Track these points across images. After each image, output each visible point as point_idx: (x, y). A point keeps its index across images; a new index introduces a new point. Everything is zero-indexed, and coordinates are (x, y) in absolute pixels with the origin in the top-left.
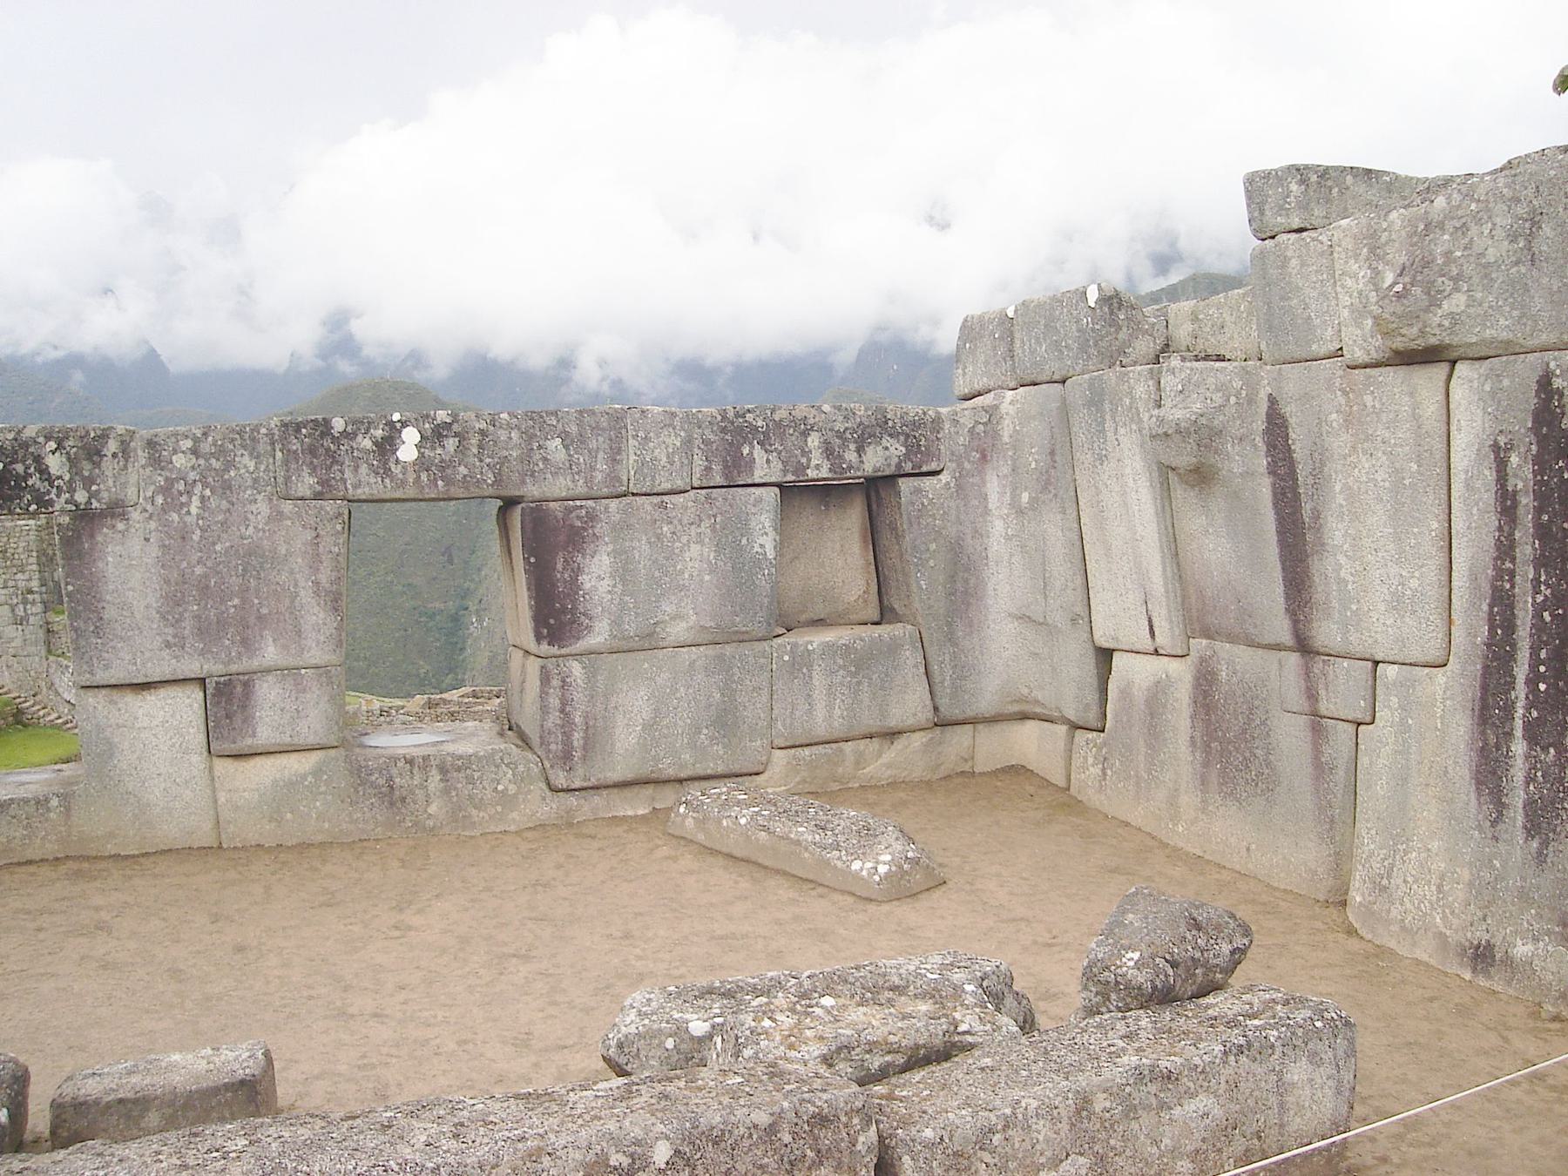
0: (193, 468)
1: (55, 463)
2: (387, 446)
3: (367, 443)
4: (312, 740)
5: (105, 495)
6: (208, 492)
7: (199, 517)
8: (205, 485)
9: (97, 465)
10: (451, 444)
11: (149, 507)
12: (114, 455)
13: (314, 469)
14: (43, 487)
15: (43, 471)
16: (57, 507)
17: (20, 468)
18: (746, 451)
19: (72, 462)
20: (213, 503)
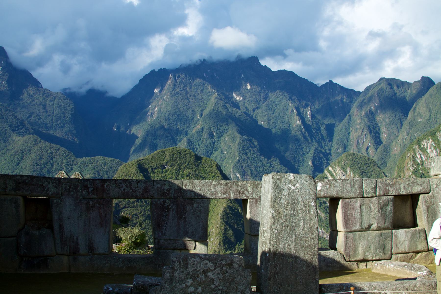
9: (257, 189)
15: (247, 190)
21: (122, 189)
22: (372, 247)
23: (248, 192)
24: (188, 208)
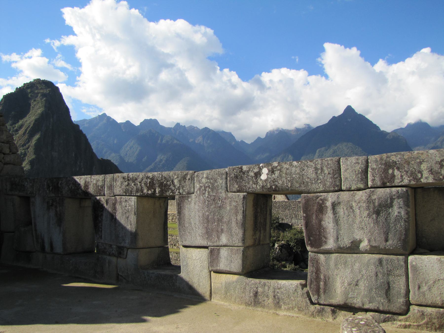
0: (206, 183)
1: (176, 181)
2: (258, 174)
3: (252, 174)
4: (235, 270)
5: (186, 191)
6: (210, 190)
7: (208, 197)
8: (209, 188)
9: (185, 182)
10: (277, 173)
11: (196, 195)
12: (189, 179)
13: (237, 184)
14: (173, 188)
16: (176, 194)
17: (169, 183)
18: (390, 171)
19: (180, 181)
20: (211, 194)
21: (70, 187)
22: (361, 283)
23: (175, 186)
24: (117, 207)
